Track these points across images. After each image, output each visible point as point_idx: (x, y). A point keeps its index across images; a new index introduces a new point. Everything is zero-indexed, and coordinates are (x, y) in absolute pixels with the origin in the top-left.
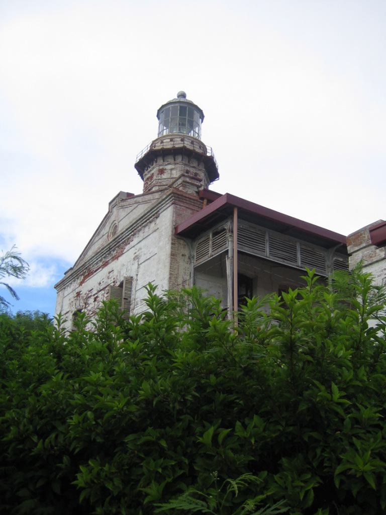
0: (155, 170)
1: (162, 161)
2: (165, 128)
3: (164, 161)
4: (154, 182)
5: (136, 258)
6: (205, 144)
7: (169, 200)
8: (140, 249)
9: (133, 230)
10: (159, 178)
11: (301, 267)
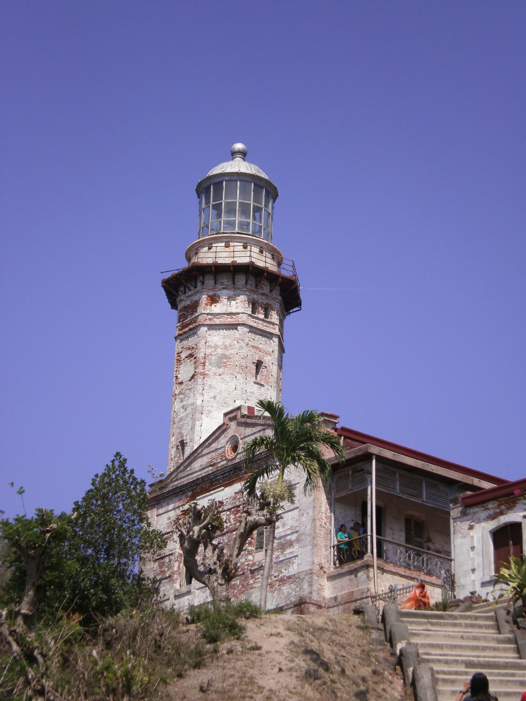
3: (215, 283)
10: (208, 311)
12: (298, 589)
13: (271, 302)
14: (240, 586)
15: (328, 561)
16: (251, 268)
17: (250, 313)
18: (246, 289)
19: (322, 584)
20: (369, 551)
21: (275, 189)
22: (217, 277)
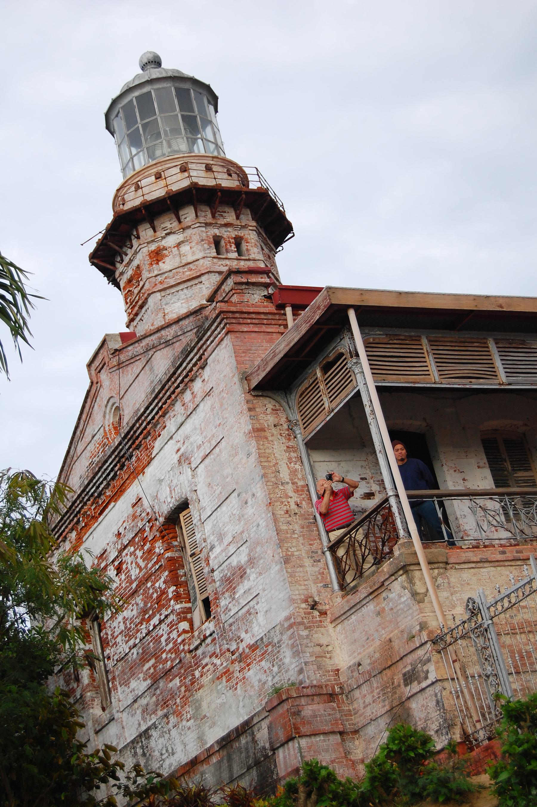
0: (139, 256)
1: (150, 232)
2: (134, 151)
3: (155, 231)
4: (147, 286)
5: (184, 459)
6: (241, 165)
7: (217, 327)
8: (187, 437)
9: (160, 404)
10: (156, 273)
11: (510, 384)
12: (275, 669)
13: (241, 233)
14: (183, 689)
15: (326, 586)
16: (194, 192)
17: (215, 254)
18: (198, 225)
19: (324, 641)
20: (402, 533)
21: (207, 88)
22: (155, 222)
